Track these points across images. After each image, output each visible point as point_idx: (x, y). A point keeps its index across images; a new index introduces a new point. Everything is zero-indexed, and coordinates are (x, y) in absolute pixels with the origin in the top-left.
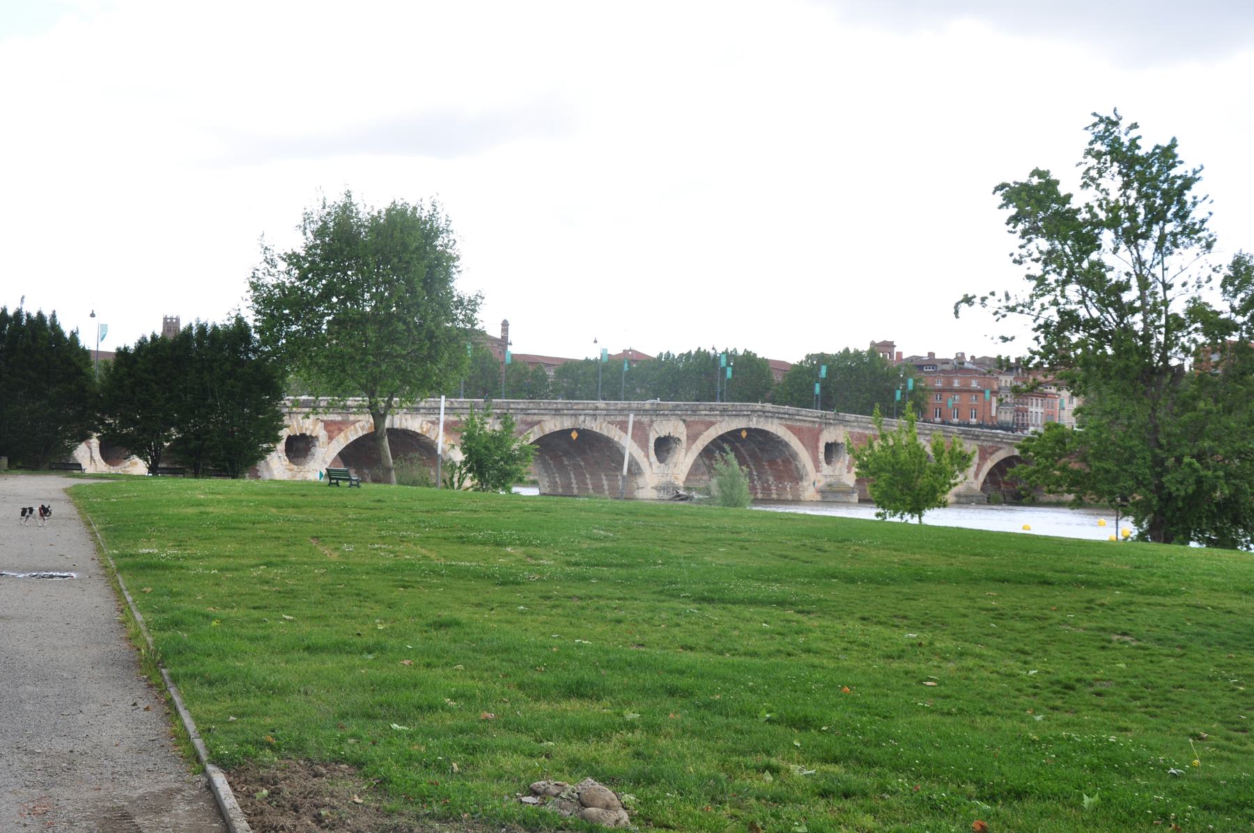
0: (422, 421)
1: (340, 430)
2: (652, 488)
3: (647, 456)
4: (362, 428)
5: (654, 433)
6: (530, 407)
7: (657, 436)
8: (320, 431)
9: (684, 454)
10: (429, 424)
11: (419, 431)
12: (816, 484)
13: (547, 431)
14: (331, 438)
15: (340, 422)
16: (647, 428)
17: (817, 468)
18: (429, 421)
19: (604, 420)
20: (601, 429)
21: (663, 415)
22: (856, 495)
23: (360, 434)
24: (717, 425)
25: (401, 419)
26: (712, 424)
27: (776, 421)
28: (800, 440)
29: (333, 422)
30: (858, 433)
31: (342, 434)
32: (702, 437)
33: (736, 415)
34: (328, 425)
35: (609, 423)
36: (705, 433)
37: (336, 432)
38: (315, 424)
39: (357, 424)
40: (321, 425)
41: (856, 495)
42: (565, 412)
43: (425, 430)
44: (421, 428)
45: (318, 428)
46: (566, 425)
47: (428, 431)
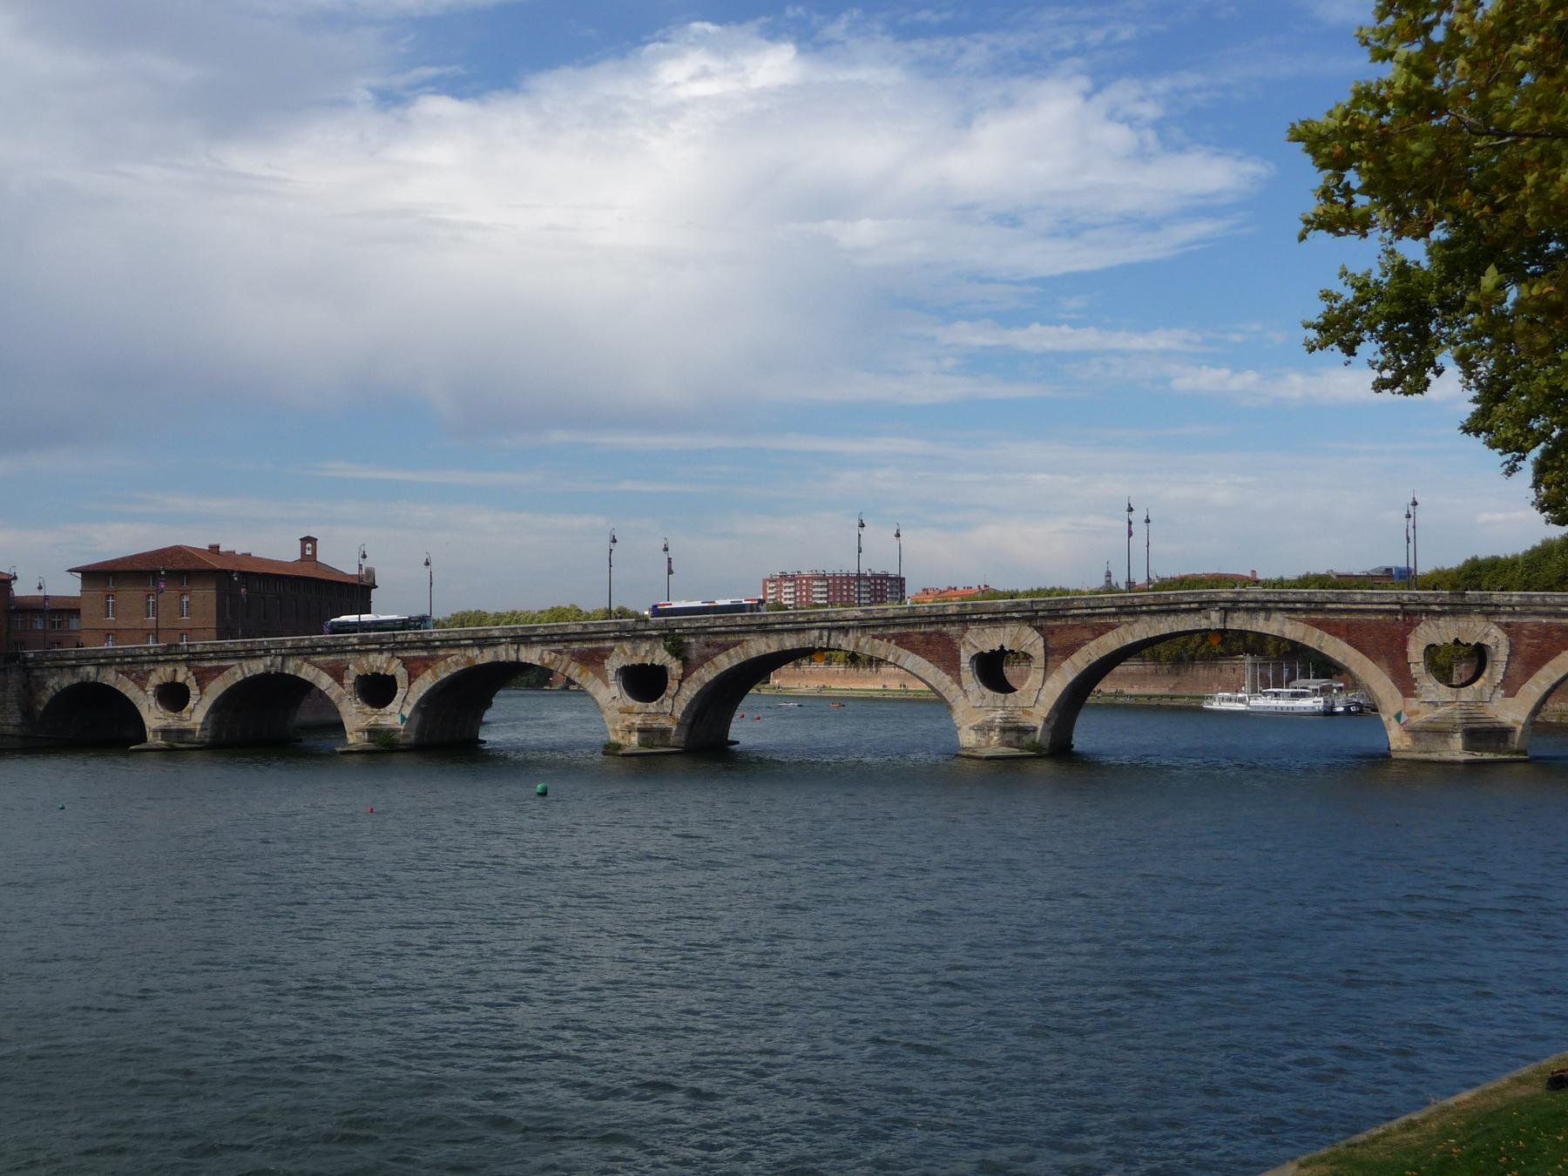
0: (543, 651)
1: (427, 667)
2: (972, 728)
3: (959, 683)
4: (457, 663)
5: (969, 647)
6: (718, 624)
7: (974, 652)
8: (397, 669)
9: (1041, 676)
10: (553, 654)
11: (538, 663)
12: (1404, 718)
13: (754, 654)
14: (412, 677)
15: (425, 658)
16: (957, 641)
17: (1407, 686)
18: (554, 651)
19: (864, 634)
21: (980, 621)
22: (1458, 735)
23: (454, 670)
24: (1121, 630)
25: (507, 650)
26: (1111, 627)
27: (1278, 616)
28: (1349, 642)
29: (415, 658)
30: (1540, 625)
31: (429, 671)
33: (990, 621)
34: (406, 662)
35: (874, 637)
36: (1093, 644)
37: (422, 669)
38: (389, 661)
39: (449, 660)
41: (1458, 735)
42: (777, 626)
43: (546, 661)
44: (541, 658)
45: (393, 666)
46: (788, 644)
47: (552, 662)
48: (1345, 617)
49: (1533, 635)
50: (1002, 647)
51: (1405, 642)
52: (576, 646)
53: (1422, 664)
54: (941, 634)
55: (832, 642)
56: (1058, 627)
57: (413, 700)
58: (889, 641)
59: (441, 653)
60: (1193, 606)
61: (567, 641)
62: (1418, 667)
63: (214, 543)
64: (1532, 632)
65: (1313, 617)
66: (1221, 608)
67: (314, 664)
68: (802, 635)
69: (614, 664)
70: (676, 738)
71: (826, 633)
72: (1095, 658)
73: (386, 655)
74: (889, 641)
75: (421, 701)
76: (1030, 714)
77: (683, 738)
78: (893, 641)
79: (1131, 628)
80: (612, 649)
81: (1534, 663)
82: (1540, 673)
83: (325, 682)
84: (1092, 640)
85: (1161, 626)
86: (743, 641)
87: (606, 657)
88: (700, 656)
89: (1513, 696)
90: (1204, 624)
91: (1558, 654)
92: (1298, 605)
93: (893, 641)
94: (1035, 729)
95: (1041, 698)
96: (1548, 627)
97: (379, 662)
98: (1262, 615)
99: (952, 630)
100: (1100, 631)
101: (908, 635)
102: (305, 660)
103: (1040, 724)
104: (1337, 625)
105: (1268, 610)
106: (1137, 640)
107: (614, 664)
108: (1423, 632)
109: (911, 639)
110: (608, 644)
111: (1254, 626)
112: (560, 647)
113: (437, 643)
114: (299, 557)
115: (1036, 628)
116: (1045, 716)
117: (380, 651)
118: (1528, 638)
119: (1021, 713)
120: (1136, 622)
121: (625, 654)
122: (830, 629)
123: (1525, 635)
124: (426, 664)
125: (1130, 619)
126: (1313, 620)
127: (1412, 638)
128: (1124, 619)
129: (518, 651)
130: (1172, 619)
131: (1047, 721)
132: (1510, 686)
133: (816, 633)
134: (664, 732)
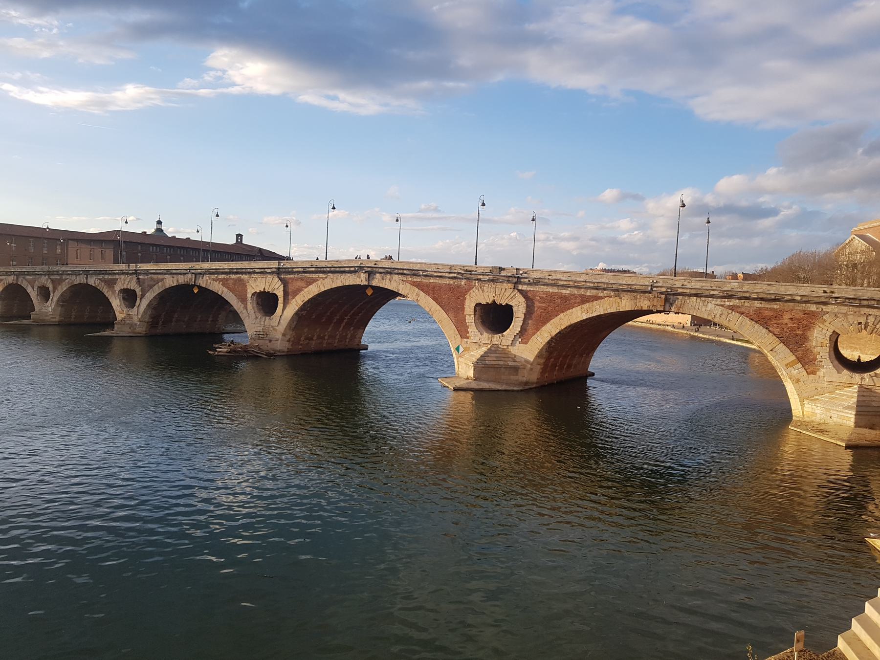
1: (60, 284)
3: (247, 310)
11: (94, 285)
14: (55, 289)
15: (59, 280)
17: (463, 332)
18: (99, 279)
20: (206, 284)
24: (319, 282)
26: (315, 280)
28: (434, 299)
30: (547, 293)
31: (60, 286)
32: (303, 292)
34: (53, 281)
40: (50, 280)
44: (95, 283)
48: (431, 281)
49: (542, 300)
50: (264, 289)
51: (465, 299)
52: (106, 277)
53: (473, 316)
54: (240, 280)
55: (197, 282)
56: (290, 279)
57: (55, 299)
58: (219, 283)
59: (64, 277)
60: (352, 269)
61: (103, 274)
62: (470, 320)
63: (145, 230)
64: (542, 298)
65: (415, 280)
66: (366, 272)
67: (26, 280)
68: (186, 276)
69: (118, 288)
70: (141, 329)
71: (194, 276)
72: (306, 300)
73: (47, 277)
74: (219, 283)
75: (58, 300)
76: (276, 330)
77: (144, 329)
78: (221, 283)
79: (324, 281)
80: (117, 279)
81: (544, 321)
82: (544, 328)
83: (29, 290)
84: (306, 288)
85: (338, 281)
86: (163, 279)
87: (115, 284)
88: (148, 286)
89: (526, 343)
90: (357, 281)
91: (556, 316)
92: (405, 272)
93: (221, 283)
94: (277, 340)
95: (282, 321)
96: (552, 296)
97: (45, 281)
98: (388, 276)
99: (245, 277)
100: (310, 282)
101: (227, 280)
102: (24, 278)
103: (279, 336)
104: (428, 286)
105: (391, 273)
106: (327, 289)
107: (118, 288)
108: (474, 294)
109: (228, 282)
110: (117, 277)
111: (383, 284)
112: (101, 277)
113: (61, 272)
114: (235, 242)
115: (280, 279)
116: (283, 332)
117: (45, 275)
118: (540, 302)
119: (272, 329)
120: (326, 278)
121: (121, 283)
122: (196, 274)
123: (537, 300)
124: (60, 281)
125: (324, 276)
126: (414, 282)
127: (467, 297)
128: (321, 275)
129: (87, 279)
130: (343, 276)
131: (284, 335)
132: (523, 335)
133: (190, 275)
134: (132, 326)
